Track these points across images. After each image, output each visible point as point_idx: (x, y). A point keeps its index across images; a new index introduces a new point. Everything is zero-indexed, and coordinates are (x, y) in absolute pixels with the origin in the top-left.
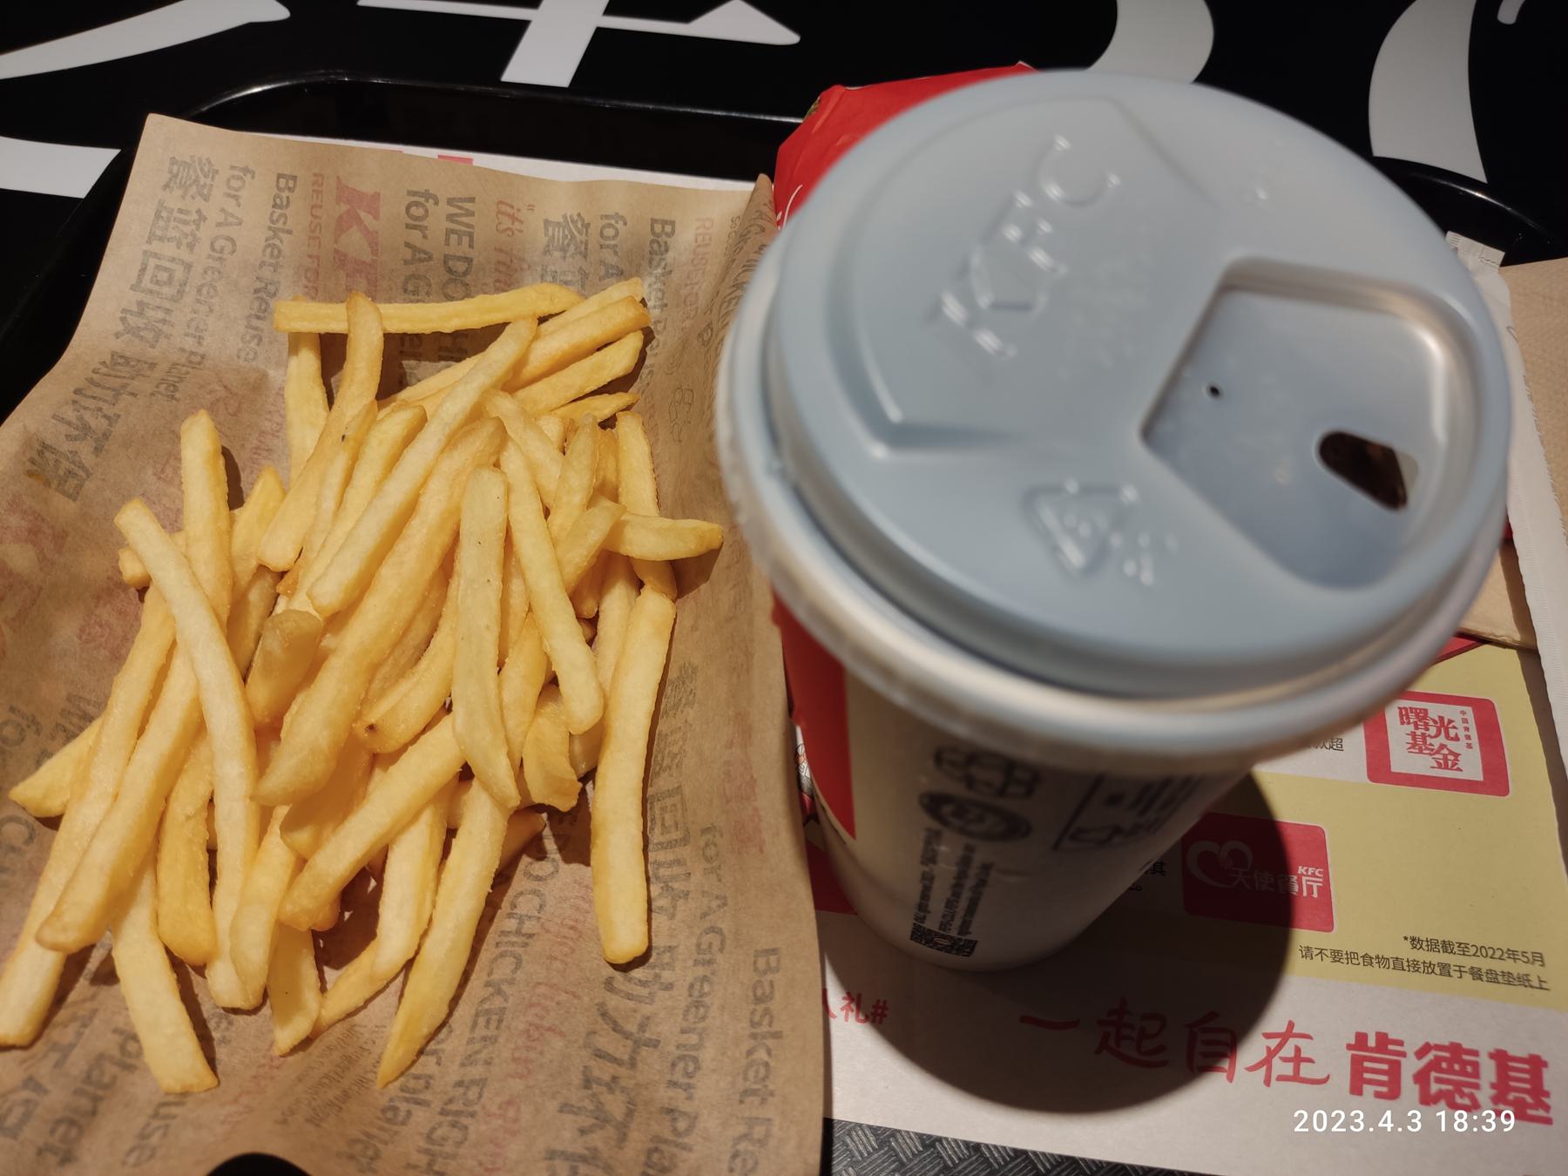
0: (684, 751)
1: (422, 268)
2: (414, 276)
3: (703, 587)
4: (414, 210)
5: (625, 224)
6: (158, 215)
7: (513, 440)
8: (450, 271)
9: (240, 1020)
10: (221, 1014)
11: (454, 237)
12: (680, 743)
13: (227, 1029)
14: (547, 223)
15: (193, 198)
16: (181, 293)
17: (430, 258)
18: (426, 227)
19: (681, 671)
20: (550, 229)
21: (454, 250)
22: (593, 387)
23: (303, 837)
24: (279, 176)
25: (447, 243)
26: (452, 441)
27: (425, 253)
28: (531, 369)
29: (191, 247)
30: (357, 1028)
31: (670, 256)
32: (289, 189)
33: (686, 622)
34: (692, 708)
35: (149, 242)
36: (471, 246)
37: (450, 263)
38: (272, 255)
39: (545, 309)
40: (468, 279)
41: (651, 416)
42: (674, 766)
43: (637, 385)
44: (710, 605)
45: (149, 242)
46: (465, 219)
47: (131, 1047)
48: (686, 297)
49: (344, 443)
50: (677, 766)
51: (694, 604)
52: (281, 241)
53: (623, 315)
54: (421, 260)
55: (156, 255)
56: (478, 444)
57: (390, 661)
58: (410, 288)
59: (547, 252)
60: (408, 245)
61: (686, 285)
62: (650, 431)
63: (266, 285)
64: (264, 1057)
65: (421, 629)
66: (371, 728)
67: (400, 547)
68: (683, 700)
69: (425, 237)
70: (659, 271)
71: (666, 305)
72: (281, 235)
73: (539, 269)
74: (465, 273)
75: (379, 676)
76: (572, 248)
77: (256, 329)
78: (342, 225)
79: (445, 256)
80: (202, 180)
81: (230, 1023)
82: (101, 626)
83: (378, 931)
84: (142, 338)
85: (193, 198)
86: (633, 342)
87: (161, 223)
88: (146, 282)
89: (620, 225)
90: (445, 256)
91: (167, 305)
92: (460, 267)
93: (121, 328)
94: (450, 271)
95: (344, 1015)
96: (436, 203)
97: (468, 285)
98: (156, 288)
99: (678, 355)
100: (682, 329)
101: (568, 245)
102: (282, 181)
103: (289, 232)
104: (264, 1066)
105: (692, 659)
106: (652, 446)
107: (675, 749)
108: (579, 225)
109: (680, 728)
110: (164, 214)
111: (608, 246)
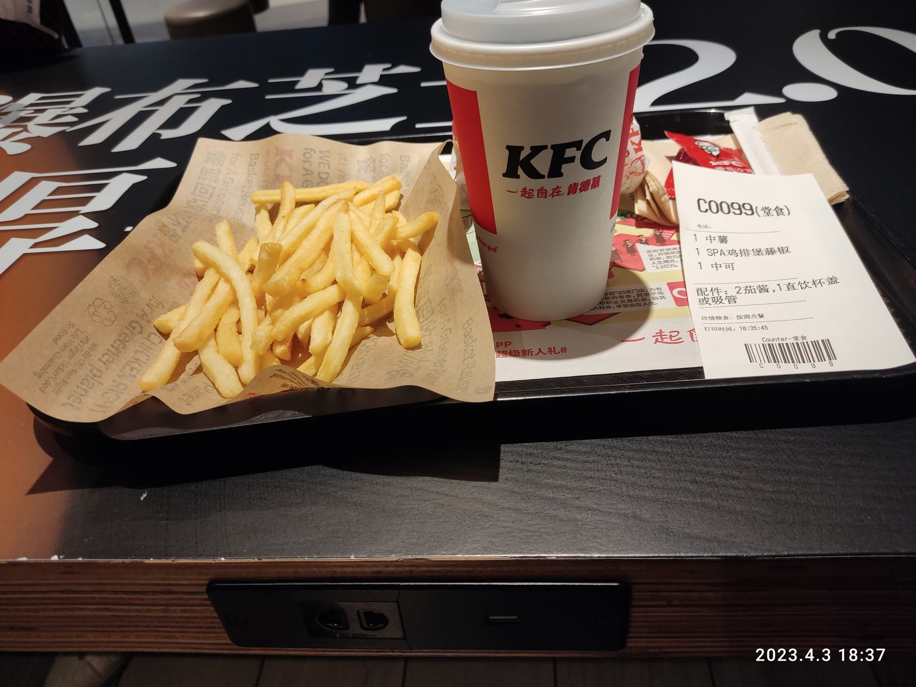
4: (306, 155)
5: (390, 157)
6: (202, 171)
7: (352, 210)
11: (322, 165)
14: (358, 162)
15: (216, 165)
16: (211, 196)
17: (313, 173)
18: (311, 161)
20: (360, 164)
24: (252, 155)
25: (319, 167)
27: (310, 171)
29: (215, 181)
31: (408, 169)
32: (256, 159)
35: (199, 179)
36: (329, 168)
37: (321, 175)
38: (248, 183)
39: (359, 187)
45: (199, 179)
46: (326, 159)
52: (252, 178)
54: (309, 174)
55: (201, 184)
59: (359, 171)
60: (304, 168)
63: (246, 194)
70: (405, 174)
71: (409, 185)
72: (252, 175)
74: (326, 179)
77: (241, 209)
78: (277, 164)
79: (319, 172)
80: (220, 159)
84: (195, 209)
85: (216, 165)
87: (203, 173)
88: (197, 192)
89: (388, 157)
90: (319, 172)
91: (206, 200)
92: (324, 176)
93: (187, 205)
94: (320, 178)
96: (315, 152)
98: (201, 194)
101: (367, 168)
102: (253, 157)
103: (256, 174)
108: (371, 161)
110: (205, 170)
111: (383, 166)
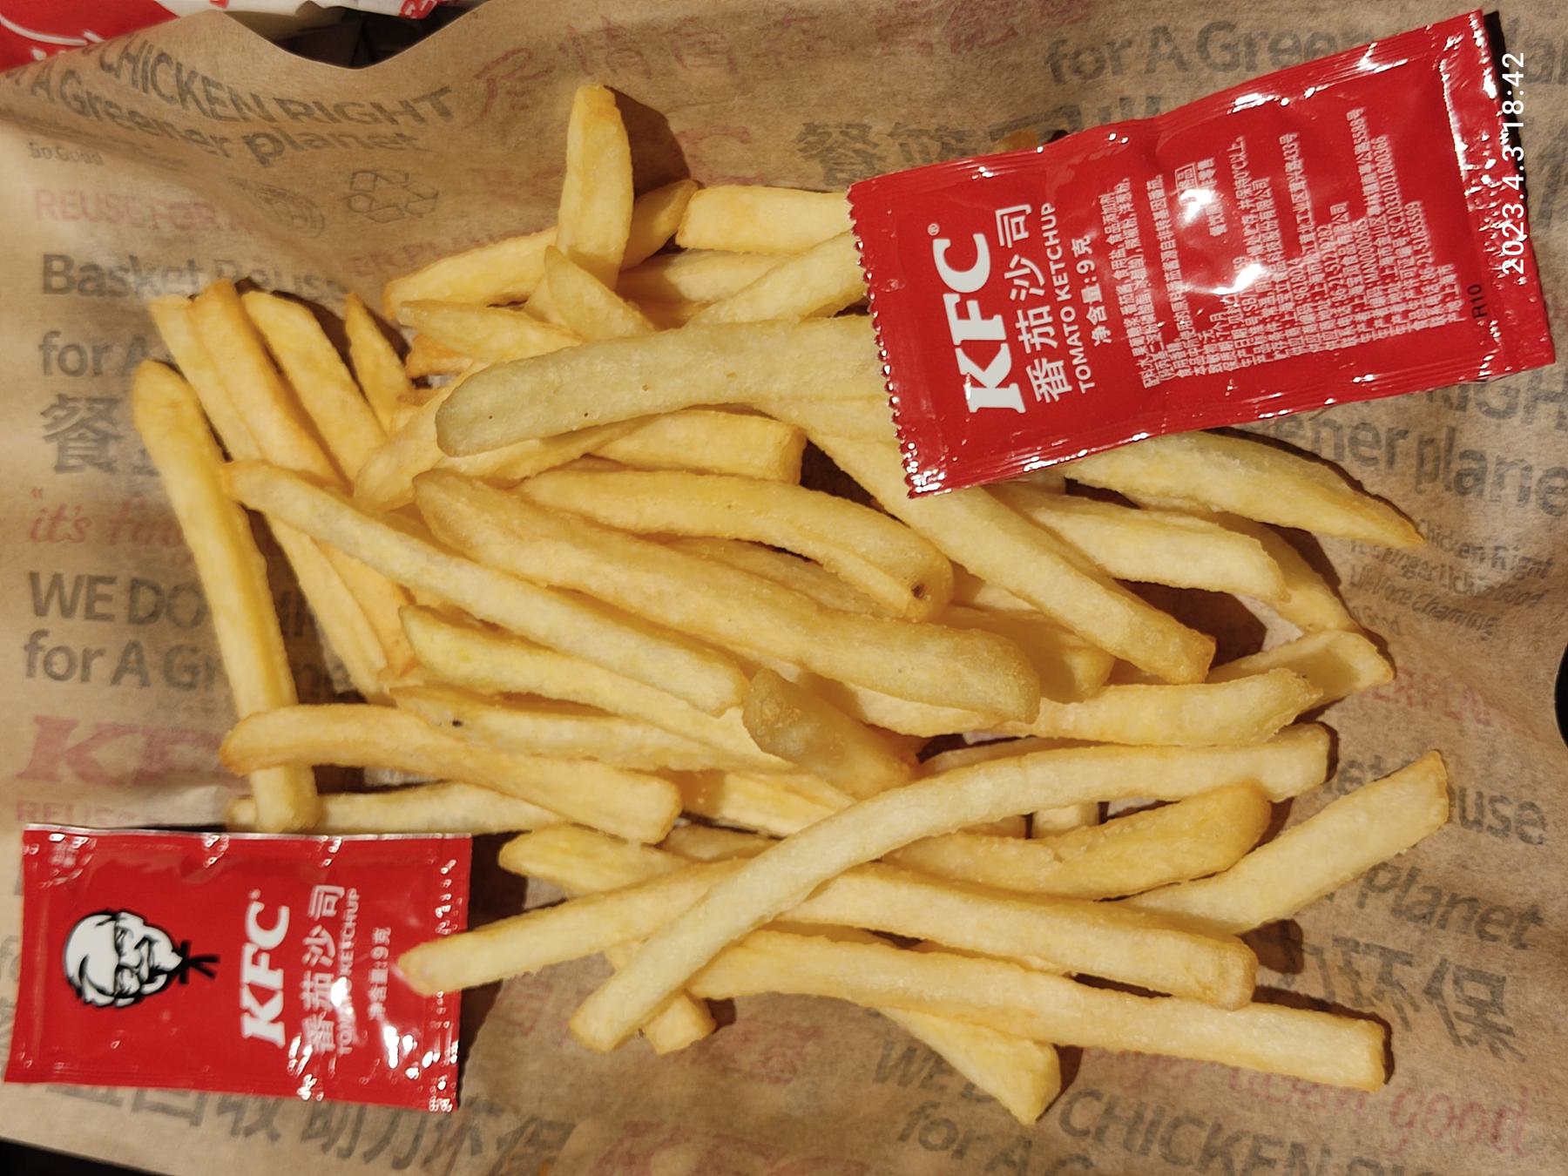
0: (937, 130)
1: (151, 658)
2: (167, 674)
3: (675, 126)
8: (154, 615)
9: (1345, 752)
10: (1340, 780)
11: (99, 607)
12: (925, 139)
13: (1360, 766)
17: (134, 645)
19: (812, 157)
21: (119, 608)
22: (342, 370)
23: (1083, 667)
26: (457, 549)
27: (126, 653)
28: (317, 465)
30: (1356, 579)
33: (733, 151)
34: (870, 128)
36: (110, 580)
40: (165, 586)
41: (391, 262)
42: (961, 145)
43: (330, 304)
44: (706, 107)
47: (1383, 878)
48: (177, 226)
49: (466, 722)
50: (960, 140)
51: (705, 141)
53: (218, 321)
54: (140, 661)
56: (460, 506)
57: (813, 593)
58: (186, 678)
59: (108, 467)
60: (116, 679)
61: (156, 227)
62: (415, 258)
64: (1397, 701)
65: (763, 560)
66: (918, 591)
67: (634, 601)
68: (859, 146)
69: (100, 653)
73: (140, 478)
74: (156, 590)
75: (838, 603)
76: (101, 425)
81: (1352, 764)
82: (769, 1059)
83: (1216, 589)
86: (263, 307)
92: (146, 598)
94: (154, 615)
95: (1336, 599)
97: (176, 589)
99: (292, 208)
100: (233, 228)
104: (1409, 698)
105: (793, 137)
106: (439, 254)
107: (935, 147)
109: (901, 145)
